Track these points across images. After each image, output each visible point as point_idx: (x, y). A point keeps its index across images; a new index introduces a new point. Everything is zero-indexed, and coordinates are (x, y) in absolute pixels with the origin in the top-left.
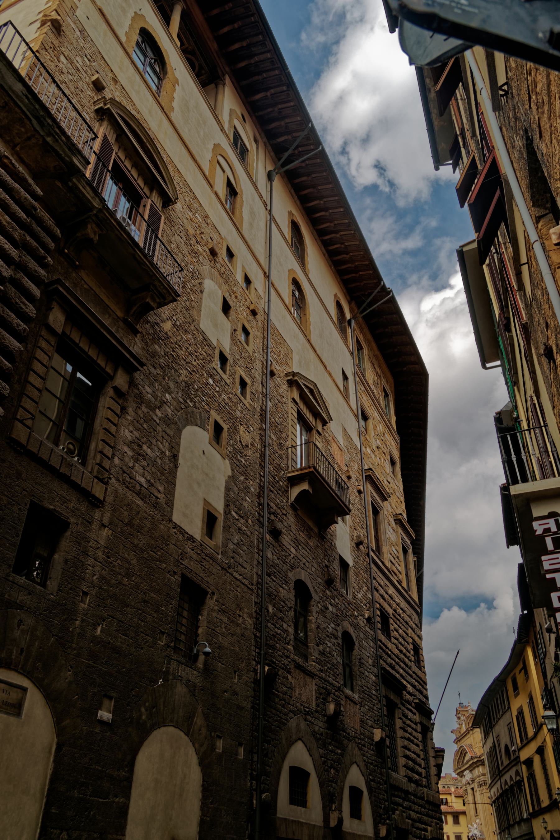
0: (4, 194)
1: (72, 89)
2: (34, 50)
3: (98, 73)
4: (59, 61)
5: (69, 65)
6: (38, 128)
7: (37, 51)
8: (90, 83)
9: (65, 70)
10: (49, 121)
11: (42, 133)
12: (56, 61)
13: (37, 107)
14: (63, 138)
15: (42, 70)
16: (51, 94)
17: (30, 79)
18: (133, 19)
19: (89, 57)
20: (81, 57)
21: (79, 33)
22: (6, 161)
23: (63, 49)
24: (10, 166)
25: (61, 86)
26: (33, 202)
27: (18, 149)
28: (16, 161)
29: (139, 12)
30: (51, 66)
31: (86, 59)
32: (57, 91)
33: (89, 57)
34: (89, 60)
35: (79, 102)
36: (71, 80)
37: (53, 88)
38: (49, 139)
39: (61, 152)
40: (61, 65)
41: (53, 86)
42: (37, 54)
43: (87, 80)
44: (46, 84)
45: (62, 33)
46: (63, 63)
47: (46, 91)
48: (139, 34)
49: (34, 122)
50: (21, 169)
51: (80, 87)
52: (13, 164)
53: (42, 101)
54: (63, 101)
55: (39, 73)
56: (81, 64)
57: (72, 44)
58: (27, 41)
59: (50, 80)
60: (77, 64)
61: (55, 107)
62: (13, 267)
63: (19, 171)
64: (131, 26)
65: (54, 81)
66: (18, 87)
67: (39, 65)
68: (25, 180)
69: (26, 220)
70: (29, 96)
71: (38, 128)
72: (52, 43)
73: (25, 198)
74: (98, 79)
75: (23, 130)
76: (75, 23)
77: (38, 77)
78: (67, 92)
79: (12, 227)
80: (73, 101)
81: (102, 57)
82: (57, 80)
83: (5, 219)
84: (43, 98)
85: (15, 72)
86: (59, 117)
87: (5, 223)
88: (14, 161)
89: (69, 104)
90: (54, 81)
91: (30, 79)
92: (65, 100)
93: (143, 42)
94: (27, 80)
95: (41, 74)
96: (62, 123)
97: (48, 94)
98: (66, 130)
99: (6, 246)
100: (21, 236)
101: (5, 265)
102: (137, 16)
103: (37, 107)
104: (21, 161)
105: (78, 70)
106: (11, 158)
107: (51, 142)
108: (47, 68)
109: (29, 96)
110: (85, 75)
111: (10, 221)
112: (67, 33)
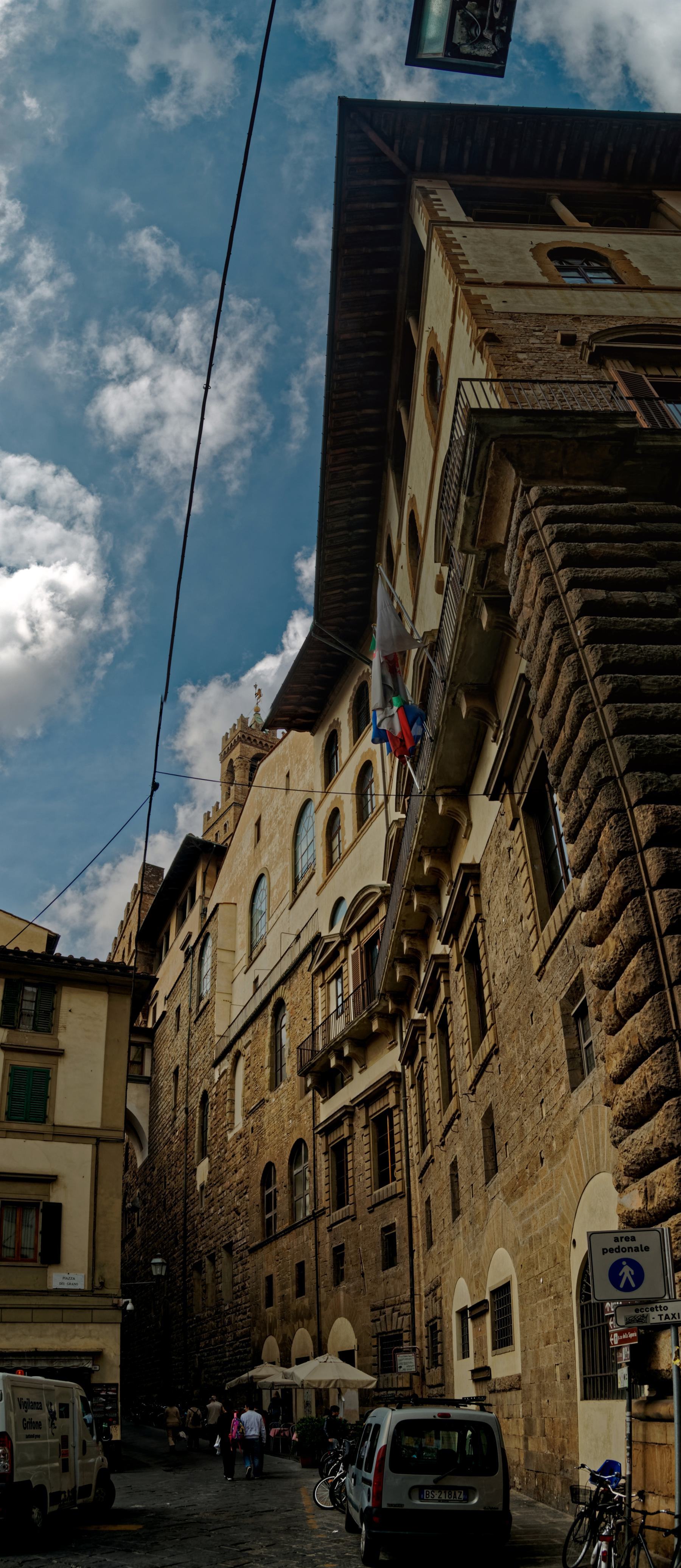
0: (594, 525)
1: (553, 369)
2: (496, 377)
3: (557, 331)
4: (521, 362)
5: (531, 354)
6: (563, 435)
7: (499, 375)
8: (561, 346)
9: (532, 362)
10: (565, 418)
11: (570, 436)
12: (518, 364)
13: (544, 419)
14: (590, 419)
15: (518, 385)
16: (542, 395)
17: (516, 403)
18: (535, 257)
19: (537, 329)
20: (532, 336)
21: (511, 322)
22: (567, 494)
23: (514, 349)
24: (575, 494)
25: (543, 378)
26: (625, 505)
27: (565, 472)
28: (575, 484)
29: (533, 247)
30: (519, 373)
31: (537, 333)
32: (544, 387)
33: (537, 329)
34: (540, 331)
35: (569, 373)
36: (545, 365)
37: (539, 389)
38: (580, 434)
39: (602, 433)
40: (525, 363)
41: (537, 386)
42: (501, 378)
43: (556, 348)
44: (531, 392)
45: (500, 338)
46: (525, 359)
47: (537, 398)
48: (552, 260)
49: (555, 434)
50: (585, 487)
51: (556, 360)
52: (575, 491)
53: (542, 410)
54: (557, 389)
55: (517, 391)
56: (538, 341)
57: (515, 336)
58: (484, 377)
59: (529, 385)
60: (536, 346)
61: (556, 402)
62: (669, 588)
63: (585, 491)
64: (540, 264)
65: (535, 382)
66: (515, 421)
67: (511, 384)
68: (600, 492)
69: (635, 529)
70: (529, 418)
71: (563, 435)
72: (502, 355)
73: (616, 509)
74: (563, 336)
75: (553, 451)
76: (500, 318)
77: (520, 394)
78: (551, 377)
79: (632, 549)
80: (564, 379)
81: (547, 315)
82: (534, 378)
83: (618, 548)
84: (540, 406)
85: (500, 412)
86: (568, 405)
87: (621, 552)
88: (573, 487)
89: (564, 386)
90: (535, 382)
91: (516, 403)
92: (557, 385)
93: (561, 263)
94: (515, 407)
95: (520, 389)
96: (575, 407)
97: (540, 398)
98: (585, 408)
99: (643, 573)
100: (647, 550)
101: (661, 594)
102: (536, 251)
103: (544, 419)
104: (579, 479)
105: (541, 349)
106: (568, 487)
107: (585, 435)
108: (519, 378)
109: (529, 418)
110: (550, 346)
111: (624, 545)
112: (503, 333)
